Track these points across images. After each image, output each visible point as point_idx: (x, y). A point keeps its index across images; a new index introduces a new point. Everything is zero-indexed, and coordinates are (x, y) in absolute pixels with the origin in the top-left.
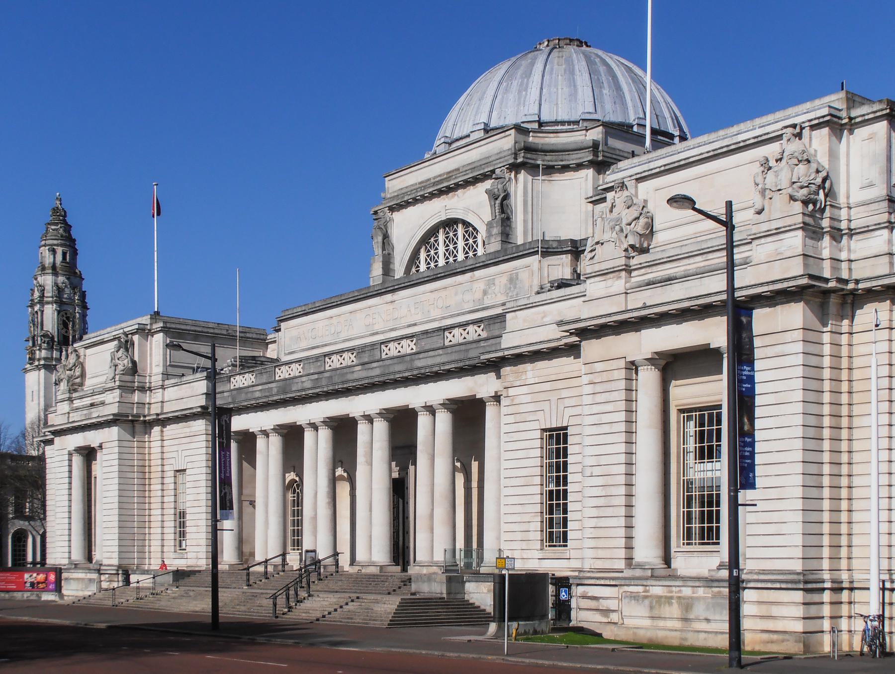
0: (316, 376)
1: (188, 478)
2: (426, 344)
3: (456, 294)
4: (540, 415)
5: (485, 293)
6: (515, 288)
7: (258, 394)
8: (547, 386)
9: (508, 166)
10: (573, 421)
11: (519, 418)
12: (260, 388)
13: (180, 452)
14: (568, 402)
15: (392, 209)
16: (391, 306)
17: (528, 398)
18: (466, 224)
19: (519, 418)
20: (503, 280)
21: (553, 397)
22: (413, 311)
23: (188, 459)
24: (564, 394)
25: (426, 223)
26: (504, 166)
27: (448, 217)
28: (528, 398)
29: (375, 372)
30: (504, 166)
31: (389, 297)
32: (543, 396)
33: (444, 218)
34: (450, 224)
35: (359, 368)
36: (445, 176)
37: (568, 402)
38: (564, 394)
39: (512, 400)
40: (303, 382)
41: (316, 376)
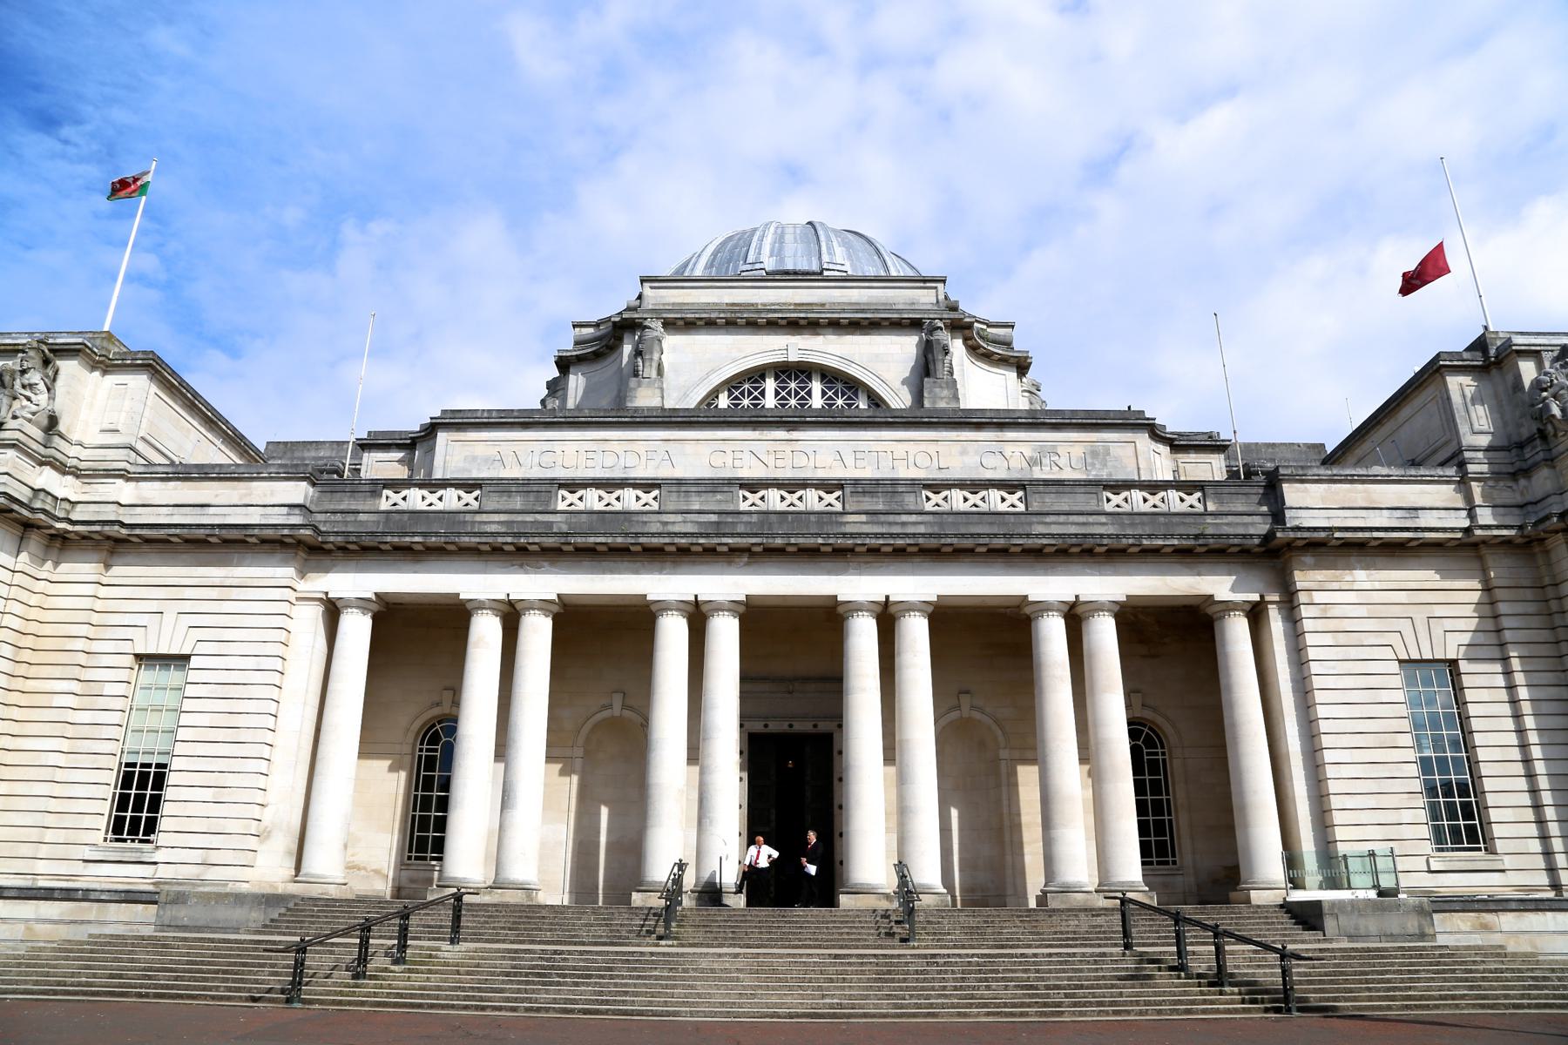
0: (714, 518)
1: (193, 676)
3: (963, 453)
4: (1394, 639)
6: (1105, 465)
12: (503, 517)
13: (169, 617)
15: (671, 325)
16: (788, 448)
18: (831, 377)
20: (1078, 451)
21: (1420, 615)
22: (849, 460)
31: (781, 434)
32: (1397, 611)
33: (793, 357)
34: (794, 372)
35: (863, 518)
36: (792, 307)
39: (1325, 610)
40: (665, 524)
41: (714, 518)
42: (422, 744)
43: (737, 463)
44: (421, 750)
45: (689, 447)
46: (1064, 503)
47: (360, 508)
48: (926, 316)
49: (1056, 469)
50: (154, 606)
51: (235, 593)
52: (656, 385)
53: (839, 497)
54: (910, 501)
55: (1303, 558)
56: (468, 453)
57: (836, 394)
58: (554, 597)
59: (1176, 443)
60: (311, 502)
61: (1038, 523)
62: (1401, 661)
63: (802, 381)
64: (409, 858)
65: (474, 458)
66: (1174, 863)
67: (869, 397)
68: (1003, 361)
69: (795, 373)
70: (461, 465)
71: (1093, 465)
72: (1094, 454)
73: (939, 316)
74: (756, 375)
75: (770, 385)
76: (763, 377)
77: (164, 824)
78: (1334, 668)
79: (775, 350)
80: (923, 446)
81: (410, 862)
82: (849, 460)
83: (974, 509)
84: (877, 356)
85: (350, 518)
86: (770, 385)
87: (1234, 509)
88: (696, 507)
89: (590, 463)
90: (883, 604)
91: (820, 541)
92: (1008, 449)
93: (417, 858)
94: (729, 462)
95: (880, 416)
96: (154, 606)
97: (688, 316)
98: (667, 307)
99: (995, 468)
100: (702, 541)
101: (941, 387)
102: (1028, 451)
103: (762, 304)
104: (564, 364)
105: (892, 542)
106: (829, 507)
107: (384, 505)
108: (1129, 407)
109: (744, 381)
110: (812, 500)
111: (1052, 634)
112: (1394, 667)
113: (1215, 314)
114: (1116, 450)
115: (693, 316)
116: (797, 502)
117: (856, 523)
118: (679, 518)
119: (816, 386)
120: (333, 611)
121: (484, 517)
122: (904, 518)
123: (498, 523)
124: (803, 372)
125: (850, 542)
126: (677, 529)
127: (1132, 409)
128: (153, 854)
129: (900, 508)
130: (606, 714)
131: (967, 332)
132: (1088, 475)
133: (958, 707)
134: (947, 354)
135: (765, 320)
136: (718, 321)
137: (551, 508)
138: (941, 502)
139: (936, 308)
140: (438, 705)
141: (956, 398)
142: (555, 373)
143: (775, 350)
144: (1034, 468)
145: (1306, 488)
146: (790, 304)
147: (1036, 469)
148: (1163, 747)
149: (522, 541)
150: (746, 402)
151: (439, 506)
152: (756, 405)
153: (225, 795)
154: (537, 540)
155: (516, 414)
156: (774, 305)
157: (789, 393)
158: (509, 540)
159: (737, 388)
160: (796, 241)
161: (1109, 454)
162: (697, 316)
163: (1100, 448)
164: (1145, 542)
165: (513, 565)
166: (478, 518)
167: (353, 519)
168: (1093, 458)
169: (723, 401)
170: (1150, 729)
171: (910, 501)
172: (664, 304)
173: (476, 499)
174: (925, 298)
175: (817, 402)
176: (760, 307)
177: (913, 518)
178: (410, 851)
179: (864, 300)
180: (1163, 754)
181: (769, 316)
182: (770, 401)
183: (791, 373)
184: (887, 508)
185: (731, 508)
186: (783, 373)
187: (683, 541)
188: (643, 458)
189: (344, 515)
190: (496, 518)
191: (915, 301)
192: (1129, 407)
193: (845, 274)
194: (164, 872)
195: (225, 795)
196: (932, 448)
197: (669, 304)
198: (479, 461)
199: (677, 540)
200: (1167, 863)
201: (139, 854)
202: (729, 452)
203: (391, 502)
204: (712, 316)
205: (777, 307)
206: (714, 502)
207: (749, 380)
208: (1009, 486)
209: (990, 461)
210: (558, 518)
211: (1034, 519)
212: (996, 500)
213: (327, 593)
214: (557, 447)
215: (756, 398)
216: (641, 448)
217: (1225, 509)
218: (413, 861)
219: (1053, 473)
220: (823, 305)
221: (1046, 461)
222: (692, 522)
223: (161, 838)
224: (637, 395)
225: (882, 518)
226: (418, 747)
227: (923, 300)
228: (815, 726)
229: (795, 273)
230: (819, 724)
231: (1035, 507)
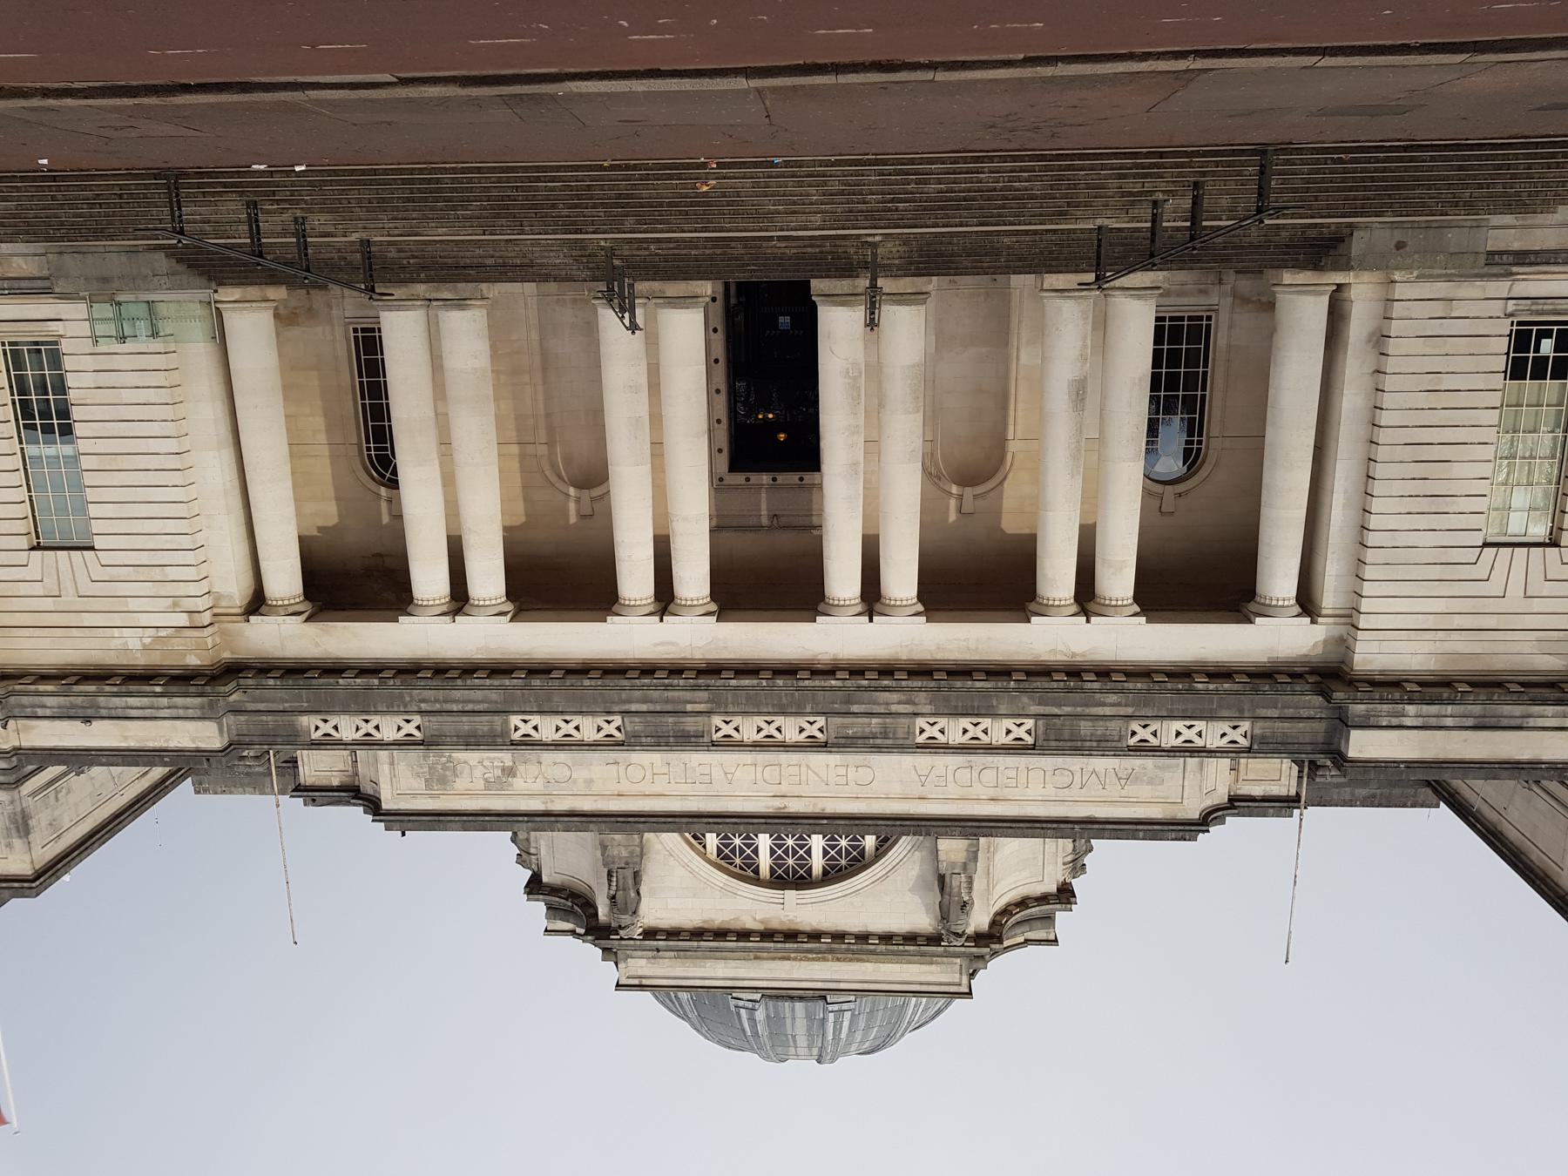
0: (855, 708)
2: (482, 724)
3: (589, 782)
5: (510, 772)
7: (1113, 698)
8: (88, 620)
9: (612, 937)
10: (22, 557)
11: (157, 574)
13: (1515, 589)
14: (37, 589)
16: (784, 789)
17: (133, 604)
18: (748, 872)
19: (157, 574)
20: (461, 784)
23: (1481, 571)
24: (48, 604)
25: (840, 894)
26: (622, 939)
27: (782, 892)
28: (133, 604)
29: (658, 695)
30: (622, 939)
31: (795, 807)
33: (791, 895)
34: (792, 878)
35: (689, 707)
37: (37, 589)
38: (48, 604)
39: (175, 605)
41: (855, 708)
42: (1199, 450)
43: (842, 771)
44: (1200, 442)
45: (897, 789)
46: (466, 724)
47: (1278, 724)
48: (638, 943)
49: (486, 763)
50: (1537, 605)
51: (1431, 622)
52: (945, 864)
53: (716, 731)
54: (634, 724)
55: (199, 663)
56: (1159, 787)
57: (742, 851)
58: (1034, 619)
59: (352, 794)
60: (1342, 730)
61: (496, 702)
62: (92, 548)
63: (780, 866)
64: (1209, 318)
65: (1151, 782)
66: (355, 330)
67: (704, 847)
68: (554, 890)
69: (789, 877)
70: (1167, 775)
71: (445, 768)
72: (443, 781)
73: (623, 942)
74: (833, 874)
75: (817, 863)
76: (825, 873)
77: (1502, 345)
78: (167, 541)
79: (812, 903)
80: (636, 789)
81: (1209, 314)
82: (717, 774)
83: (568, 718)
84: (694, 896)
85: (1290, 712)
86: (817, 863)
87: (278, 718)
88: (874, 721)
89: (1012, 773)
90: (666, 613)
91: (733, 682)
92: (539, 786)
93: (1201, 318)
94: (851, 771)
95: (691, 823)
96: (1537, 605)
97: (912, 948)
98: (939, 959)
99: (555, 764)
100: (865, 683)
101: (620, 858)
102: (518, 783)
103: (828, 960)
104: (1065, 894)
105: (655, 681)
106: (728, 719)
107: (1245, 726)
108: (403, 834)
109: (846, 868)
110: (749, 728)
111: (487, 579)
112: (98, 542)
113: (296, 943)
114: (419, 785)
115: (907, 948)
116: (764, 725)
117: (697, 701)
118: (894, 708)
119: (765, 862)
120: (1307, 603)
121: (1123, 711)
122: (644, 708)
123: (1104, 705)
124: (780, 877)
125: (700, 681)
126: (895, 697)
127: (400, 833)
128: (1514, 308)
129: (649, 719)
130: (980, 489)
131: (594, 924)
132: (450, 756)
133: (593, 500)
134: (614, 897)
135: (822, 940)
136: (877, 942)
137: (1040, 723)
138: (605, 725)
139: (628, 952)
140: (1180, 495)
141: (604, 847)
142: (1077, 884)
143: (812, 903)
144: (511, 764)
145: (194, 742)
146: (795, 959)
147: (509, 763)
148: (370, 456)
149: (1072, 683)
150: (844, 843)
151: (1178, 725)
152: (779, 838)
153: (1428, 382)
154: (1055, 685)
155: (1107, 834)
156: (813, 959)
157: (795, 852)
158: (1089, 685)
159: (855, 859)
160: (794, 1037)
161: (426, 780)
162: (901, 948)
163: (436, 788)
164: (376, 682)
165: (1082, 655)
166: (1130, 711)
167: (1286, 711)
168: (445, 776)
169: (870, 842)
170: (383, 476)
171: (634, 724)
172: (943, 963)
173: (1134, 733)
174: (640, 966)
175: (764, 842)
176: (830, 957)
177: (634, 707)
178: (1208, 327)
179: (709, 963)
180: (369, 449)
181: (818, 945)
182: (817, 842)
183: (793, 877)
184: (664, 720)
185: (839, 720)
186: (802, 877)
187: (886, 682)
188: (950, 777)
189: (1298, 715)
190: (1108, 711)
191: (653, 961)
192: (403, 834)
193: (734, 995)
194: (1501, 287)
195: (1428, 382)
196: (625, 787)
197: (937, 963)
198: (1145, 778)
199: (894, 683)
200: (363, 330)
201: (1533, 308)
202: (852, 784)
203: (1241, 731)
204: (884, 947)
205: (810, 956)
206: (856, 726)
207: (841, 869)
208: (527, 743)
209: (560, 772)
210: (1035, 709)
211: (500, 707)
212: (547, 727)
213: (1313, 622)
214: (1051, 792)
215: (833, 847)
216: (953, 791)
217: (286, 718)
218: (1205, 314)
219: (488, 758)
220: (756, 958)
221: (498, 772)
222: (879, 704)
223: (1505, 327)
224: (965, 853)
225: (669, 708)
226: (1203, 446)
227: (643, 962)
228: (748, 479)
229: (792, 998)
230: (744, 482)
231: (498, 719)
